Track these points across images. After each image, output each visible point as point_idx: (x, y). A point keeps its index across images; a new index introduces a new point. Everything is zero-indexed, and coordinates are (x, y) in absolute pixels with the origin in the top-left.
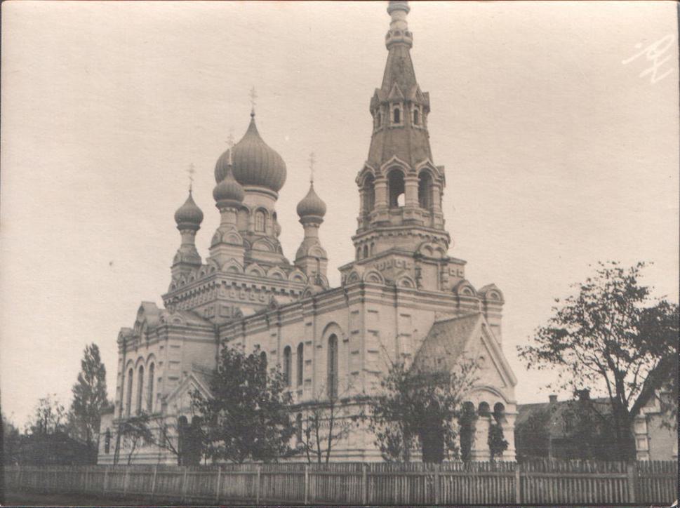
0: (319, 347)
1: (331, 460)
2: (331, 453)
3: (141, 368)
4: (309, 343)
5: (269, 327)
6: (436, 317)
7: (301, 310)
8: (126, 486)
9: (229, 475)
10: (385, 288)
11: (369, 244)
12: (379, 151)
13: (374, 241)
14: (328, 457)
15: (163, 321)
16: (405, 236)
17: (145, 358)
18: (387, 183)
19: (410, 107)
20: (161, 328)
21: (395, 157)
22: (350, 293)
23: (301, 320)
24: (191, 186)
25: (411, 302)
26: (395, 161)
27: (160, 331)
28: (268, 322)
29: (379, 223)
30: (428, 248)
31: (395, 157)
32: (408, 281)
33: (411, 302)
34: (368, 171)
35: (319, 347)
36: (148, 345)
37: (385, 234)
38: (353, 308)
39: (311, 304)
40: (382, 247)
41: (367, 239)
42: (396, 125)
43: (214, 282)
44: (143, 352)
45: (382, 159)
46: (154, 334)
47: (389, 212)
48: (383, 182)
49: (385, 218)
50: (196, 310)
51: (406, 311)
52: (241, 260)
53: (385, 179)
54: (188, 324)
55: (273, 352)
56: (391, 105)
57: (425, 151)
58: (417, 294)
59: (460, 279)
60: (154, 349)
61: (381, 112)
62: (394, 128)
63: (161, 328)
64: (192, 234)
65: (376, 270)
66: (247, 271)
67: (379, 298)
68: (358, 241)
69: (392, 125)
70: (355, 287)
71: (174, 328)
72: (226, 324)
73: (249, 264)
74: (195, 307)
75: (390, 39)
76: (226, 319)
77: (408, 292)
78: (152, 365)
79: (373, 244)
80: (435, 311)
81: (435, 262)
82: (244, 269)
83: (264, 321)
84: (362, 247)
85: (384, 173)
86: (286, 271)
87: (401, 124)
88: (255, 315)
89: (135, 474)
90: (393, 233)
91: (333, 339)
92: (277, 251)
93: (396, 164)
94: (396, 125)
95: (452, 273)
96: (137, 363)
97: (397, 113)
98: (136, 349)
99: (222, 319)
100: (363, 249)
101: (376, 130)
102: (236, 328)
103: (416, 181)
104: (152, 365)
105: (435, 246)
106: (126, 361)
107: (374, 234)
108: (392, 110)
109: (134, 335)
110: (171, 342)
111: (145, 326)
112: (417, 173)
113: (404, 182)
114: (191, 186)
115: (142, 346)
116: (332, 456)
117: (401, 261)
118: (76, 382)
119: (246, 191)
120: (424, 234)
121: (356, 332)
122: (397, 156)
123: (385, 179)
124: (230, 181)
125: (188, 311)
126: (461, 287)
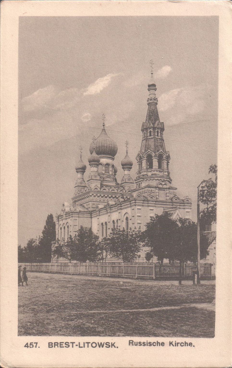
0: (123, 221)
1: (107, 261)
2: (106, 259)
3: (64, 228)
4: (119, 220)
5: (107, 213)
6: (164, 210)
7: (117, 207)
8: (55, 269)
9: (81, 266)
10: (143, 200)
11: (140, 183)
12: (144, 148)
13: (142, 182)
14: (105, 260)
15: (71, 210)
16: (153, 180)
17: (65, 223)
18: (146, 160)
19: (155, 130)
20: (70, 213)
21: (149, 150)
22: (131, 202)
23: (117, 211)
24: (81, 155)
25: (154, 205)
26: (149, 152)
27: (70, 214)
28: (107, 211)
29: (143, 175)
30: (161, 184)
31: (149, 150)
32: (152, 197)
33: (154, 205)
34: (140, 155)
35: (123, 221)
36: (66, 219)
37: (145, 179)
38: (133, 208)
39: (120, 205)
40: (143, 185)
41: (139, 181)
42: (150, 137)
43: (89, 195)
44: (65, 221)
45: (145, 151)
46: (68, 215)
47: (147, 171)
48: (145, 160)
49: (145, 173)
50: (83, 205)
51: (152, 208)
52: (99, 186)
53: (145, 159)
54: (80, 211)
55: (109, 222)
56: (148, 129)
57: (161, 147)
58: (156, 202)
59: (174, 195)
60: (69, 220)
61: (145, 132)
62: (149, 138)
63: (70, 213)
64: (82, 174)
65: (140, 194)
66: (102, 190)
67: (142, 204)
68: (137, 181)
69: (148, 137)
70: (133, 200)
71: (75, 213)
72: (93, 211)
73: (103, 187)
74: (83, 204)
75: (148, 102)
76: (94, 209)
77: (153, 201)
78: (68, 226)
79: (141, 183)
80: (164, 208)
81: (164, 189)
82: (100, 189)
83: (106, 211)
84: (138, 184)
85: (146, 156)
86: (117, 188)
87: (152, 137)
88: (104, 208)
89: (58, 266)
90: (148, 179)
91: (127, 219)
92: (114, 181)
93: (149, 153)
94: (150, 137)
95: (171, 193)
96: (63, 226)
97: (150, 132)
98: (62, 220)
99: (93, 209)
100: (138, 185)
101: (143, 139)
102: (97, 212)
103: (157, 159)
104: (68, 226)
105: (163, 183)
106: (59, 225)
107: (142, 179)
108: (149, 131)
109: (61, 215)
110: (73, 218)
111: (65, 212)
112: (157, 156)
113: (152, 159)
114: (81, 155)
115: (64, 219)
116: (107, 260)
117: (150, 190)
118: (43, 229)
119: (100, 157)
120: (159, 179)
121: (133, 216)
122: (150, 150)
123: (145, 159)
124: (95, 155)
125: (81, 205)
126: (174, 198)
